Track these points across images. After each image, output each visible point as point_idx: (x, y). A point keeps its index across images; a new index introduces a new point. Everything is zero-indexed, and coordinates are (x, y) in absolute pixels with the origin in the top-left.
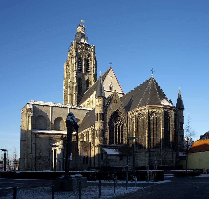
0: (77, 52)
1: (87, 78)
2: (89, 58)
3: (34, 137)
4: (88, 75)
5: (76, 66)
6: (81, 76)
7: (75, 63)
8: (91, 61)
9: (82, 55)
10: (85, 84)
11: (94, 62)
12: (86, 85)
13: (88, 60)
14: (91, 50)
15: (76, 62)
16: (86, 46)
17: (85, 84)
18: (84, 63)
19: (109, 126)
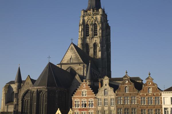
0: (84, 20)
1: (95, 42)
2: (96, 22)
3: (7, 108)
4: (96, 38)
5: (83, 33)
6: (89, 41)
7: (81, 31)
8: (98, 24)
9: (89, 21)
10: (92, 48)
11: (101, 24)
12: (93, 48)
13: (95, 24)
14: (99, 14)
15: (82, 30)
16: (93, 12)
17: (92, 48)
18: (91, 27)
19: (21, 102)
